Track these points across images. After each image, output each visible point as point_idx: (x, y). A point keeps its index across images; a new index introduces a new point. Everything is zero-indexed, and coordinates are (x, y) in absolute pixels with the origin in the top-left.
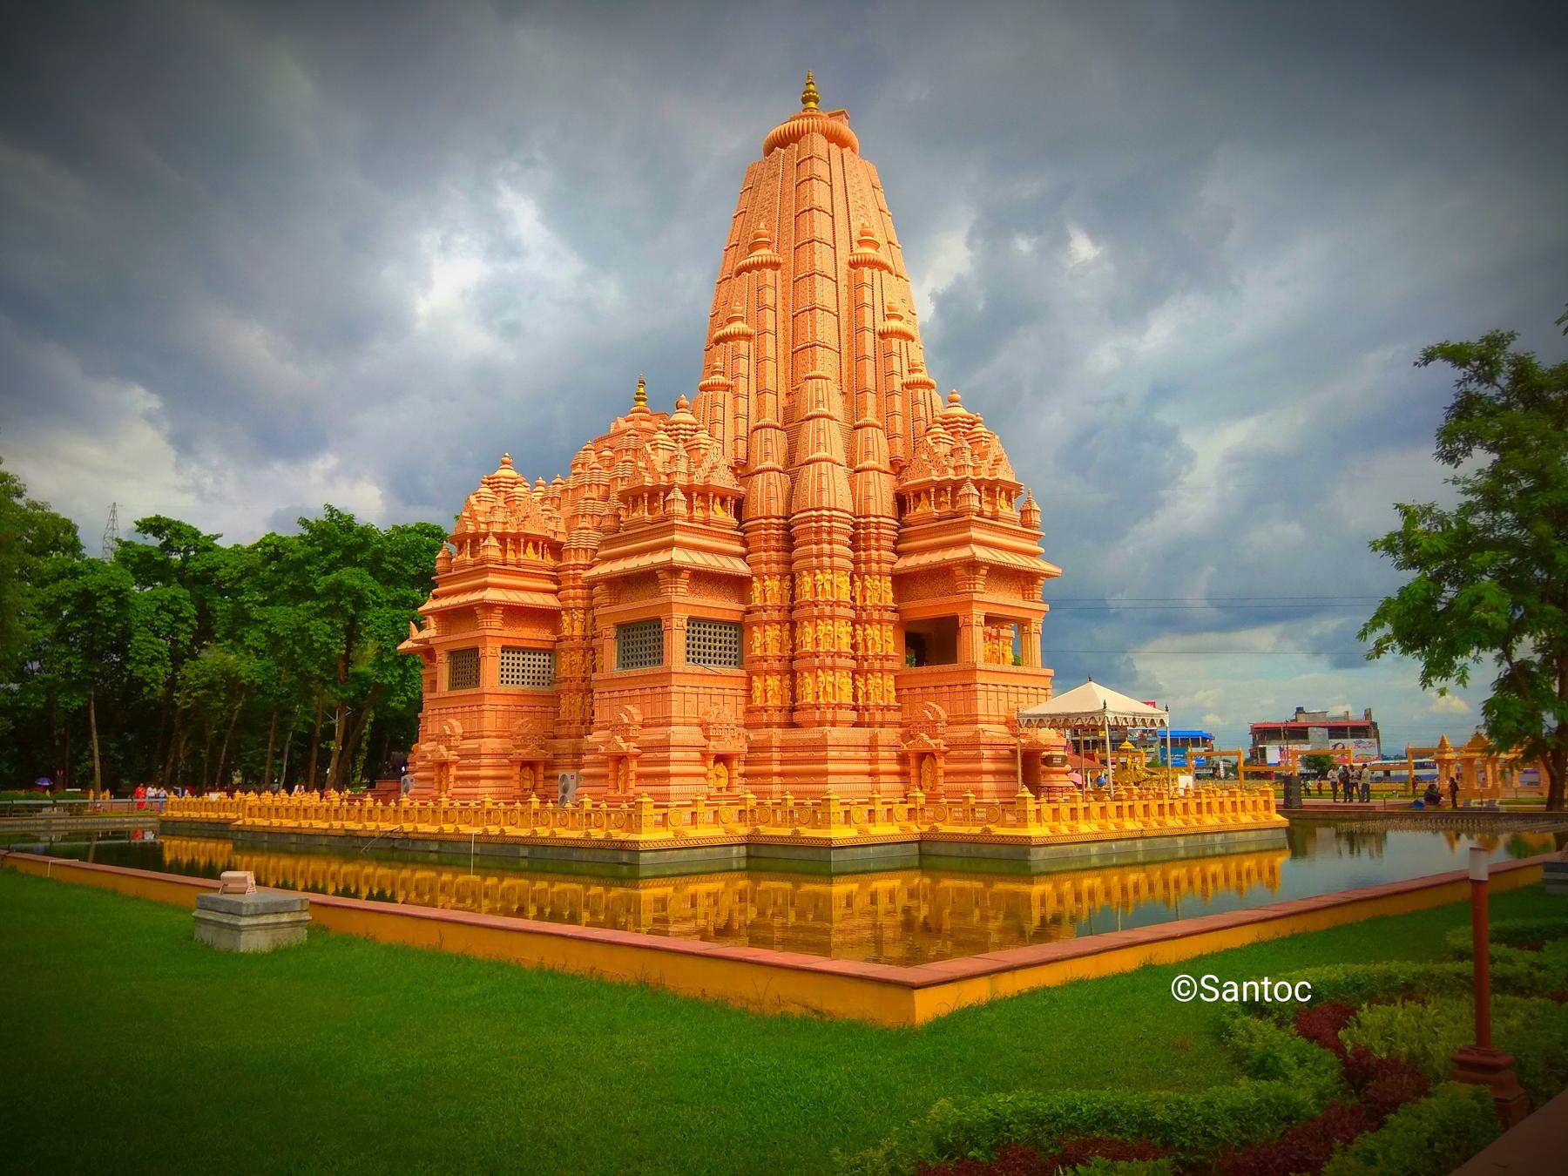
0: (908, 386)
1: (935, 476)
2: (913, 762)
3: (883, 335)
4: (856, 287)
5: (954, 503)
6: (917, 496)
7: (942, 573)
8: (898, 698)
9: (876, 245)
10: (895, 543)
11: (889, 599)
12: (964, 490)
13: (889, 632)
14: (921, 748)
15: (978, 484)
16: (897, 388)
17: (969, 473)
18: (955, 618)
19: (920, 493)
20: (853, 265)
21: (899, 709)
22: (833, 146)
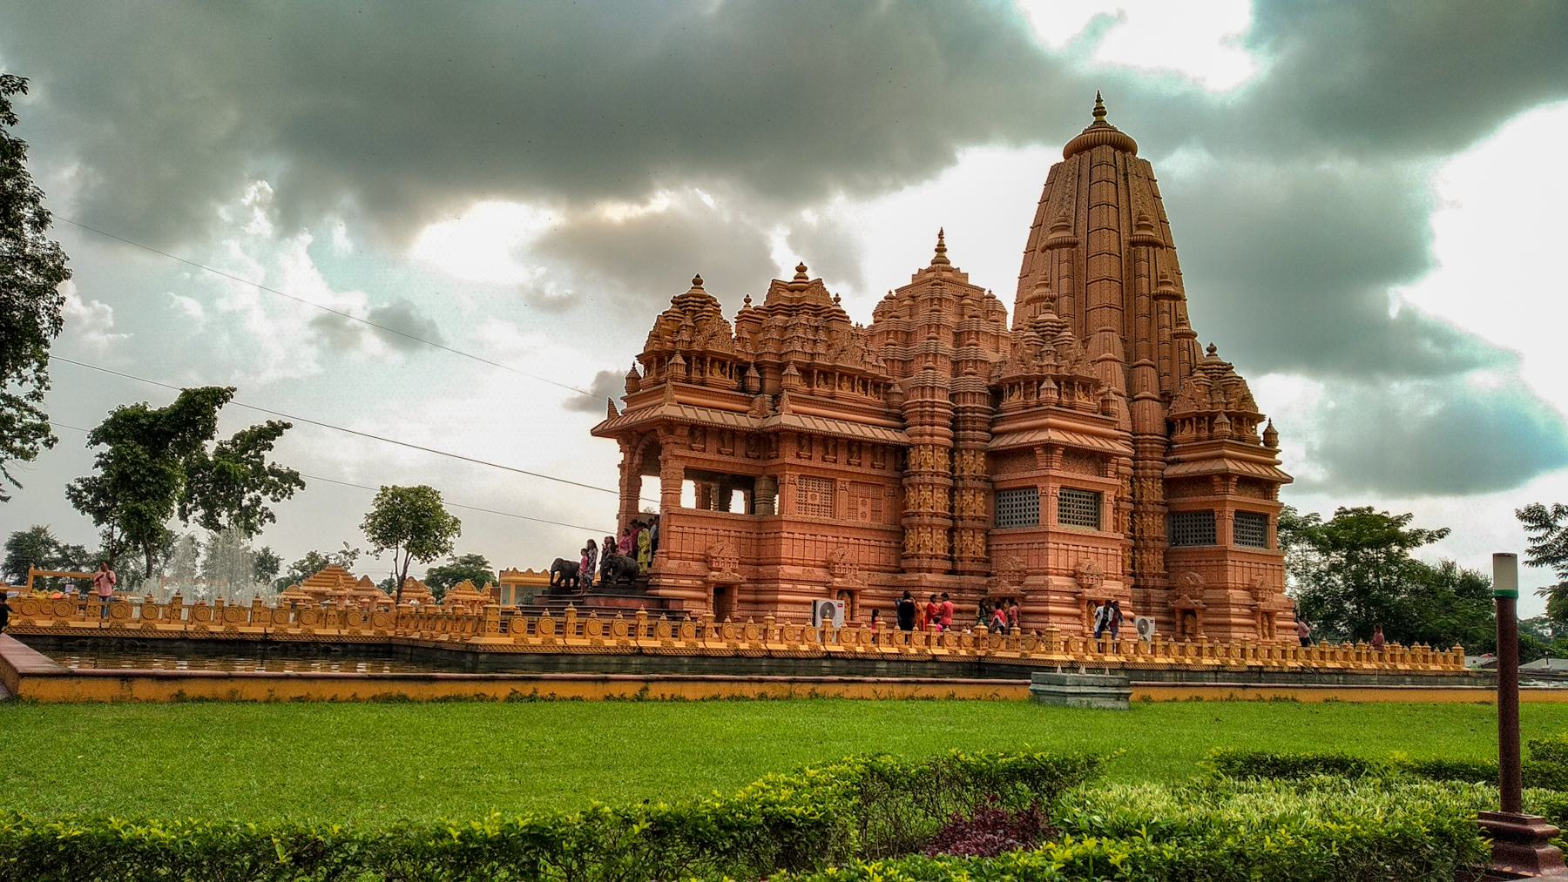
0: (1176, 336)
1: (1195, 409)
2: (1178, 616)
3: (1156, 297)
4: (1134, 260)
5: (1211, 429)
6: (1183, 422)
7: (1202, 481)
8: (1166, 568)
9: (1150, 227)
10: (1165, 454)
11: (1158, 496)
12: (1218, 420)
13: (1159, 521)
14: (1183, 605)
15: (1229, 415)
16: (1167, 338)
17: (1221, 408)
18: (1211, 513)
19: (1185, 420)
20: (1133, 244)
21: (1166, 577)
22: (1118, 153)
